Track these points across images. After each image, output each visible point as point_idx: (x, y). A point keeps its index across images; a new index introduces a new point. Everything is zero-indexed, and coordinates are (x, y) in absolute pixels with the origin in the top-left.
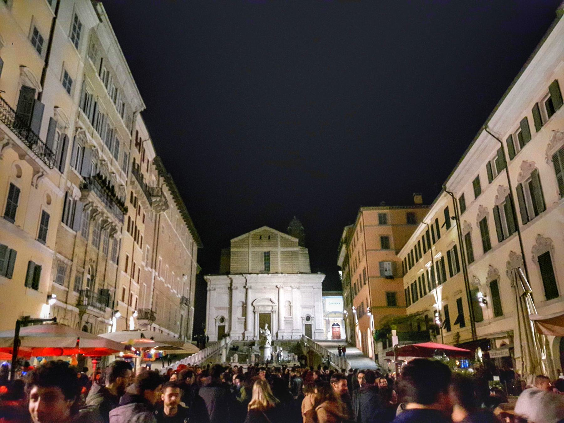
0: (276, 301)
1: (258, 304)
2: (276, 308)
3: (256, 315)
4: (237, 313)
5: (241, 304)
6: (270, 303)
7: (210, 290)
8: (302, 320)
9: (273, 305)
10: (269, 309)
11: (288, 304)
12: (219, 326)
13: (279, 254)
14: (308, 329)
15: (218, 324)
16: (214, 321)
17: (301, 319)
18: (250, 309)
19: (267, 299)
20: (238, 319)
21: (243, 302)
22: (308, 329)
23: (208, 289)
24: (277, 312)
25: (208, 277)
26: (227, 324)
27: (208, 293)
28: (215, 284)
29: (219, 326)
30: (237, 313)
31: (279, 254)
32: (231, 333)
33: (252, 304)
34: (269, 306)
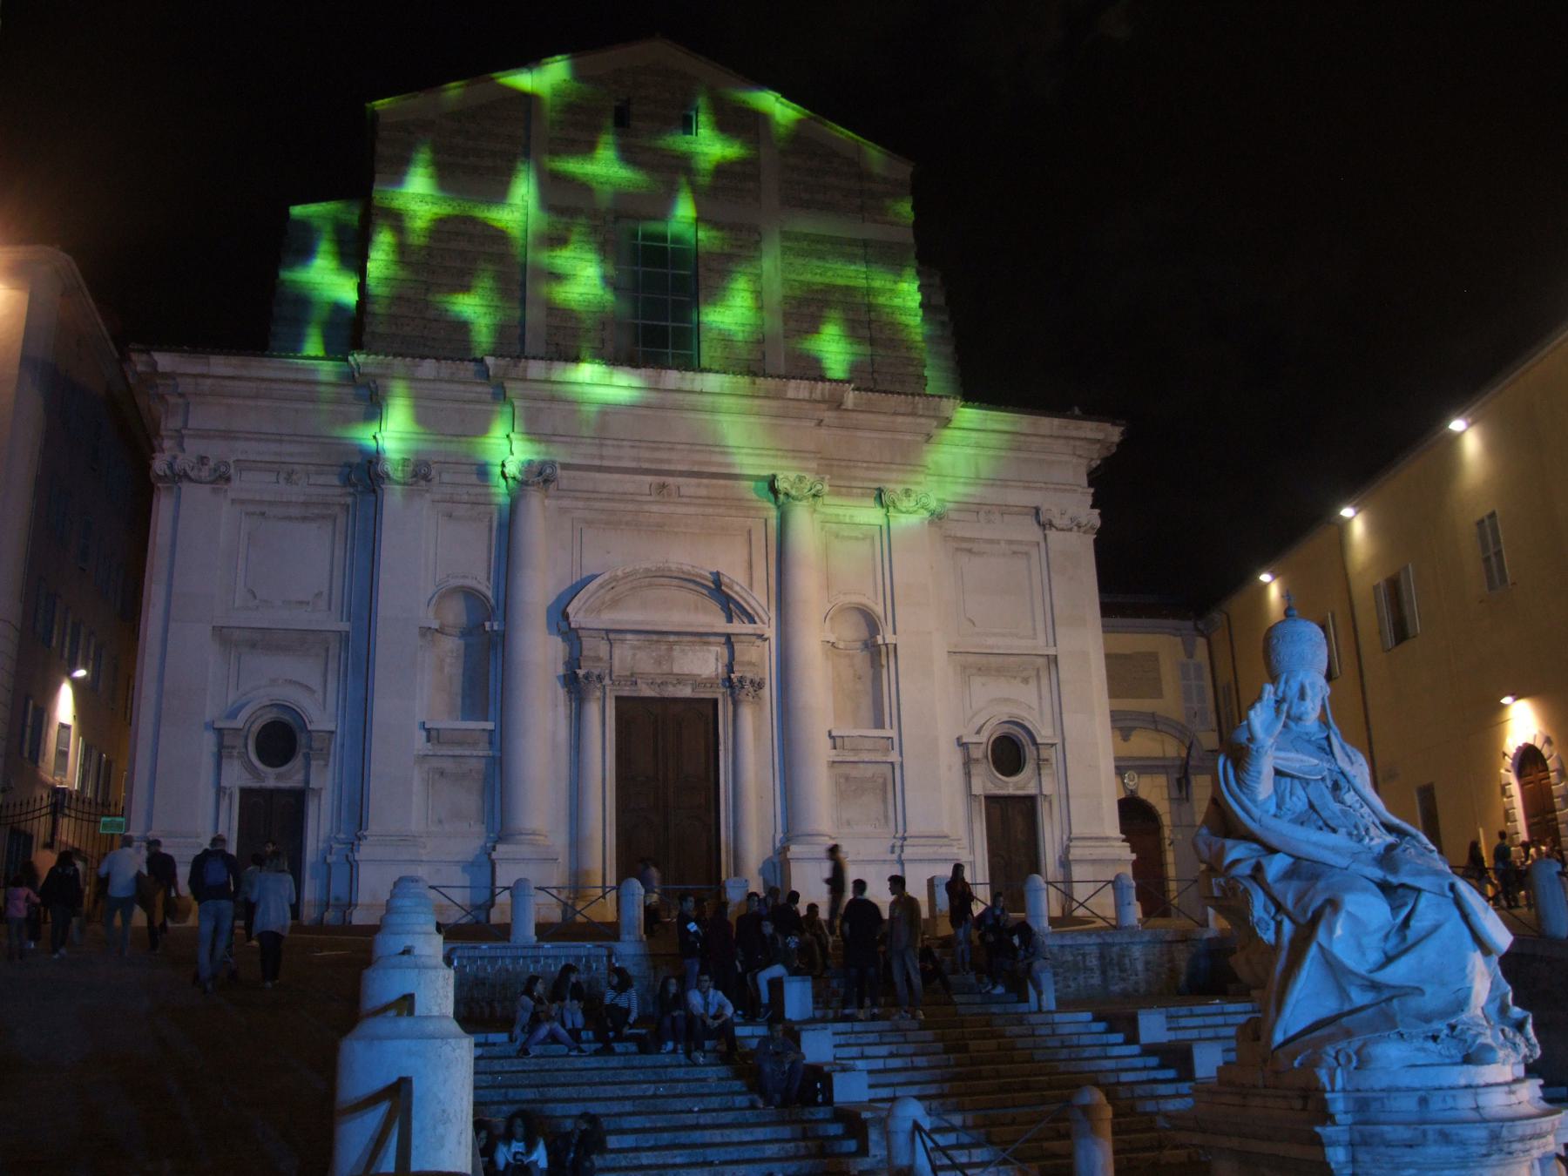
0: (759, 598)
1: (608, 618)
2: (760, 658)
3: (593, 711)
4: (417, 692)
5: (455, 613)
6: (714, 620)
7: (178, 477)
8: (968, 762)
9: (737, 627)
10: (705, 664)
11: (850, 632)
12: (246, 793)
14: (1013, 828)
15: (237, 777)
16: (209, 740)
17: (957, 758)
18: (539, 654)
19: (688, 580)
20: (431, 734)
21: (470, 594)
22: (1013, 828)
23: (159, 465)
24: (769, 693)
25: (165, 361)
26: (325, 781)
27: (163, 508)
28: (227, 435)
29: (246, 793)
30: (417, 692)
32: (364, 852)
33: (559, 618)
34: (702, 637)
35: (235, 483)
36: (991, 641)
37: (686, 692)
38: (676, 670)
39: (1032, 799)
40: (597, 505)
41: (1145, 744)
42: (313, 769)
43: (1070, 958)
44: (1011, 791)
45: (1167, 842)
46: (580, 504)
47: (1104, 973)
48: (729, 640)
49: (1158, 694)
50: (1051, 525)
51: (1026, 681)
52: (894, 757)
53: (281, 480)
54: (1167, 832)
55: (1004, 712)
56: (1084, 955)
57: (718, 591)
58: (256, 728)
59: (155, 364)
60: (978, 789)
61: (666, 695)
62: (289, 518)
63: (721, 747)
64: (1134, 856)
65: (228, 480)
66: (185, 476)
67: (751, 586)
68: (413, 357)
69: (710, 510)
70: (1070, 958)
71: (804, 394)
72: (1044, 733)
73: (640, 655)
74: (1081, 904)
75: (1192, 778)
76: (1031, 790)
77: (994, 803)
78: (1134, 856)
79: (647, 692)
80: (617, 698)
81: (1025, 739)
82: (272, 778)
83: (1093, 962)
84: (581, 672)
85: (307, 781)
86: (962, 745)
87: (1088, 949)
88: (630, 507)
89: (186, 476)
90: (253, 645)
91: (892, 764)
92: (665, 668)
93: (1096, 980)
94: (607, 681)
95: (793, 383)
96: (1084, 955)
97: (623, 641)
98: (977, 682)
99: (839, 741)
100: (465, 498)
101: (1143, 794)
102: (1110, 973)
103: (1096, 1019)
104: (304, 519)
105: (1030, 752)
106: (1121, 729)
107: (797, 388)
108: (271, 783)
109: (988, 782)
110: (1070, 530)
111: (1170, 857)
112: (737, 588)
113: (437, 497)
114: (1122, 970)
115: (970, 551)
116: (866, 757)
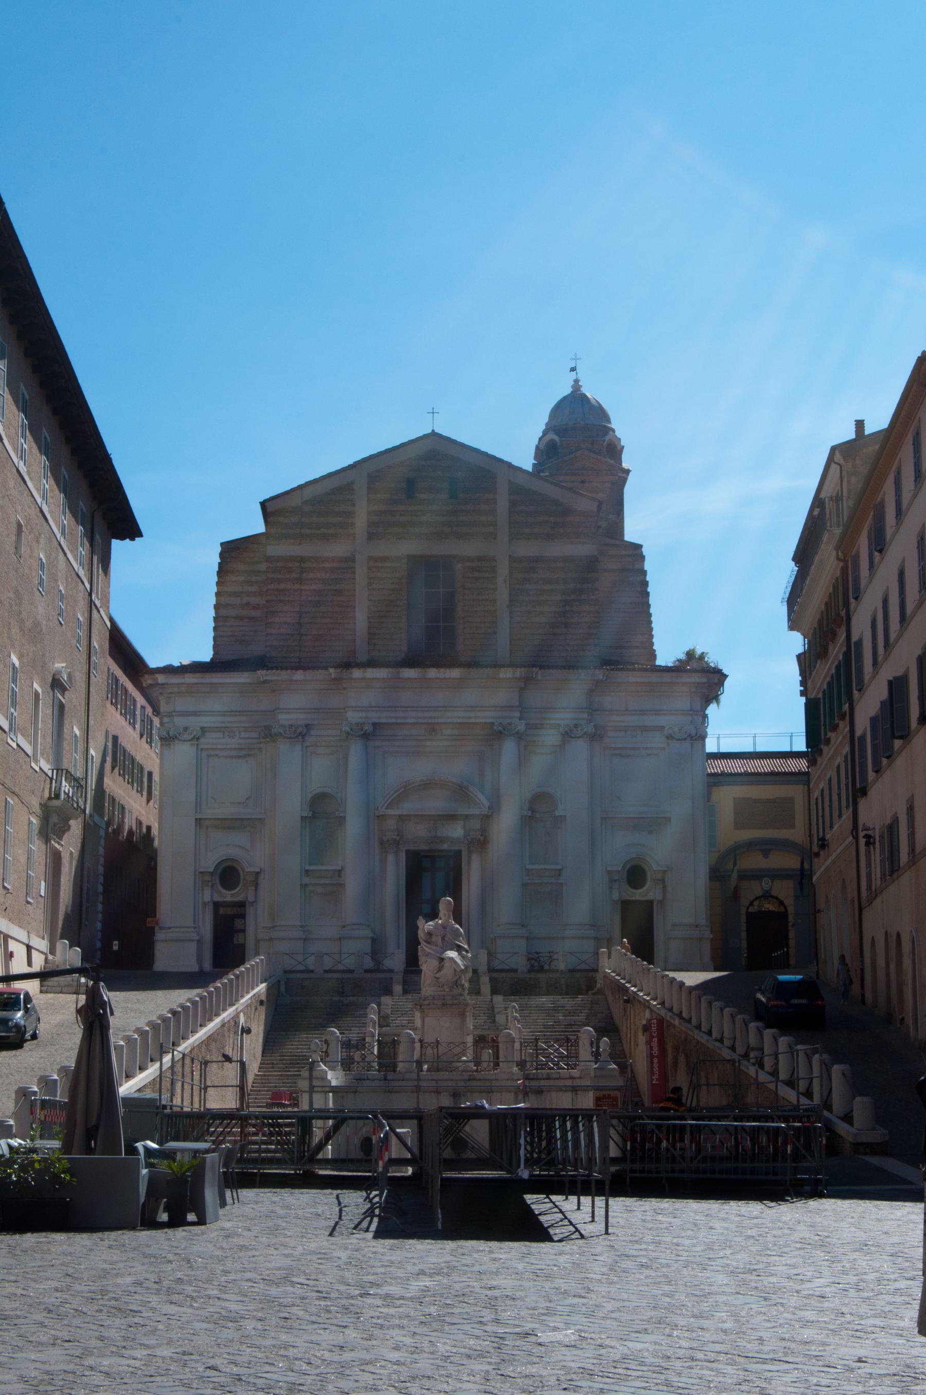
3: (391, 858)
8: (612, 881)
13: (503, 570)
28: (196, 714)
31: (503, 570)
35: (202, 740)
39: (651, 902)
44: (637, 898)
45: (790, 924)
49: (792, 826)
54: (791, 918)
59: (156, 679)
60: (616, 896)
62: (232, 757)
64: (711, 936)
65: (198, 739)
68: (292, 669)
76: (650, 897)
77: (626, 906)
78: (711, 936)
80: (407, 852)
81: (647, 869)
82: (228, 896)
84: (385, 839)
85: (247, 898)
88: (414, 743)
91: (561, 884)
95: (502, 670)
101: (774, 893)
104: (240, 757)
108: (229, 899)
110: (685, 739)
111: (792, 934)
115: (620, 755)
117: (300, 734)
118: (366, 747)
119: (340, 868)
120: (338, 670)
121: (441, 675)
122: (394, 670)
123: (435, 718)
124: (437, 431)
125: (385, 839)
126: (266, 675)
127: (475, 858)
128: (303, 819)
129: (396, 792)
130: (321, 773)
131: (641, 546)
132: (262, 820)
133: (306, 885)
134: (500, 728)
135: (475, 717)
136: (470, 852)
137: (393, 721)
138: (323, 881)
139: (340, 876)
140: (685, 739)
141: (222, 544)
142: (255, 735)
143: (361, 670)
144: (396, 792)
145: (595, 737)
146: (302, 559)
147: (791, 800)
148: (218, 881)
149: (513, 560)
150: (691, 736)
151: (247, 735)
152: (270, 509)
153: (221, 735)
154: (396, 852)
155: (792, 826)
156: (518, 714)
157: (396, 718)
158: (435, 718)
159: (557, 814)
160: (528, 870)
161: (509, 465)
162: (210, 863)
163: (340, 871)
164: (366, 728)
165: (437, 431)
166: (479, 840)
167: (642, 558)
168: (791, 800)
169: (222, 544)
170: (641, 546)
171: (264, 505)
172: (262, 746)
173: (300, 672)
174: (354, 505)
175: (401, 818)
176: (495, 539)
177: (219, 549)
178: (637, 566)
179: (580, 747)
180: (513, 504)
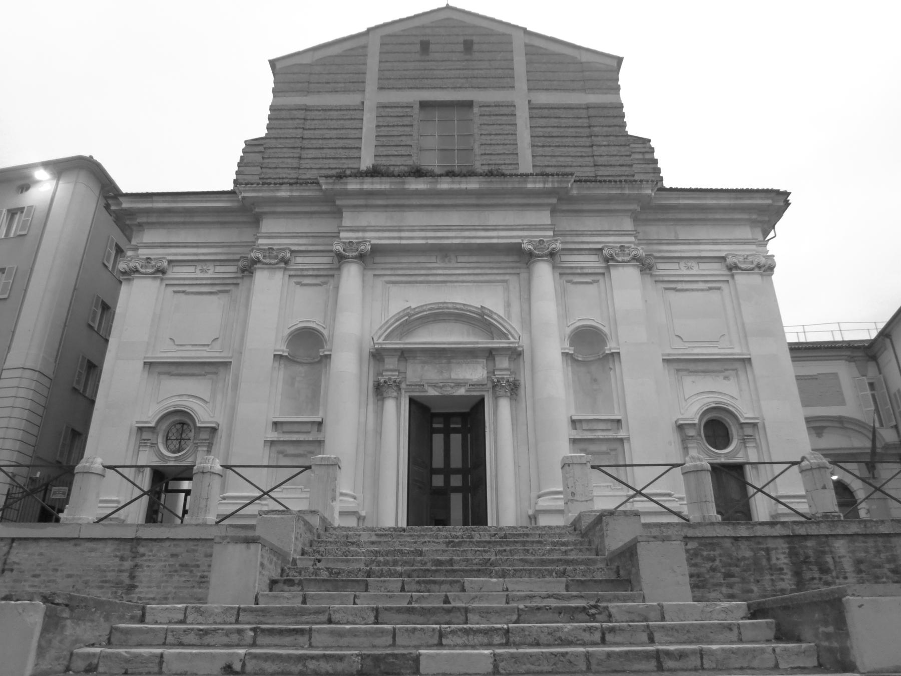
3: (390, 405)
8: (685, 441)
10: (475, 373)
15: (147, 458)
34: (469, 354)
35: (168, 276)
36: (696, 351)
37: (462, 391)
38: (453, 377)
39: (737, 469)
40: (400, 272)
41: (835, 441)
42: (200, 454)
43: (748, 554)
44: (723, 460)
46: (389, 272)
47: (797, 574)
48: (490, 354)
49: (843, 403)
50: (736, 267)
51: (726, 378)
52: (622, 434)
53: (198, 271)
55: (709, 401)
56: (768, 550)
57: (480, 321)
58: (164, 426)
61: (446, 393)
63: (487, 430)
65: (163, 272)
66: (137, 271)
67: (509, 317)
69: (478, 271)
70: (748, 554)
71: (540, 186)
72: (746, 413)
73: (426, 367)
74: (760, 490)
75: (879, 466)
76: (739, 459)
79: (432, 392)
80: (412, 401)
83: (781, 559)
86: (681, 427)
87: (771, 544)
88: (423, 272)
89: (137, 271)
90: (170, 374)
91: (621, 440)
92: (446, 375)
93: (787, 582)
94: (403, 386)
95: (530, 178)
96: (768, 550)
97: (415, 358)
98: (688, 380)
99: (578, 426)
100: (311, 273)
102: (807, 575)
103: (755, 612)
104: (211, 293)
105: (734, 431)
106: (814, 428)
107: (535, 182)
109: (702, 456)
110: (753, 269)
112: (495, 317)
113: (292, 273)
114: (824, 570)
115: (675, 289)
116: (600, 435)
117: (282, 261)
118: (363, 275)
119: (320, 420)
120: (331, 181)
121: (456, 186)
122: (398, 180)
123: (448, 238)
124: (451, 4)
125: (382, 381)
126: (245, 191)
127: (505, 405)
128: (278, 357)
129: (397, 320)
130: (305, 307)
131: (649, 141)
132: (227, 364)
133: (272, 443)
134: (530, 247)
135: (498, 237)
136: (496, 398)
137: (397, 242)
138: (295, 437)
139: (319, 430)
140: (753, 269)
141: (246, 142)
142: (232, 269)
143: (358, 180)
144: (397, 320)
145: (645, 266)
146: (307, 109)
147: (836, 374)
148: (160, 440)
149: (532, 107)
150: (759, 266)
151: (222, 269)
152: (279, 66)
153: (192, 269)
154: (397, 398)
155: (843, 403)
156: (551, 233)
157: (401, 238)
158: (448, 238)
159: (607, 352)
160: (574, 423)
161: (524, 30)
162: (150, 414)
163: (320, 424)
164: (362, 247)
165: (451, 4)
166: (508, 381)
167: (652, 150)
168: (836, 374)
169: (246, 142)
170: (649, 141)
171: (273, 63)
172: (239, 281)
173: (284, 187)
174: (365, 64)
175: (405, 355)
176: (514, 87)
177: (244, 146)
178: (647, 156)
179: (626, 278)
180: (529, 63)
